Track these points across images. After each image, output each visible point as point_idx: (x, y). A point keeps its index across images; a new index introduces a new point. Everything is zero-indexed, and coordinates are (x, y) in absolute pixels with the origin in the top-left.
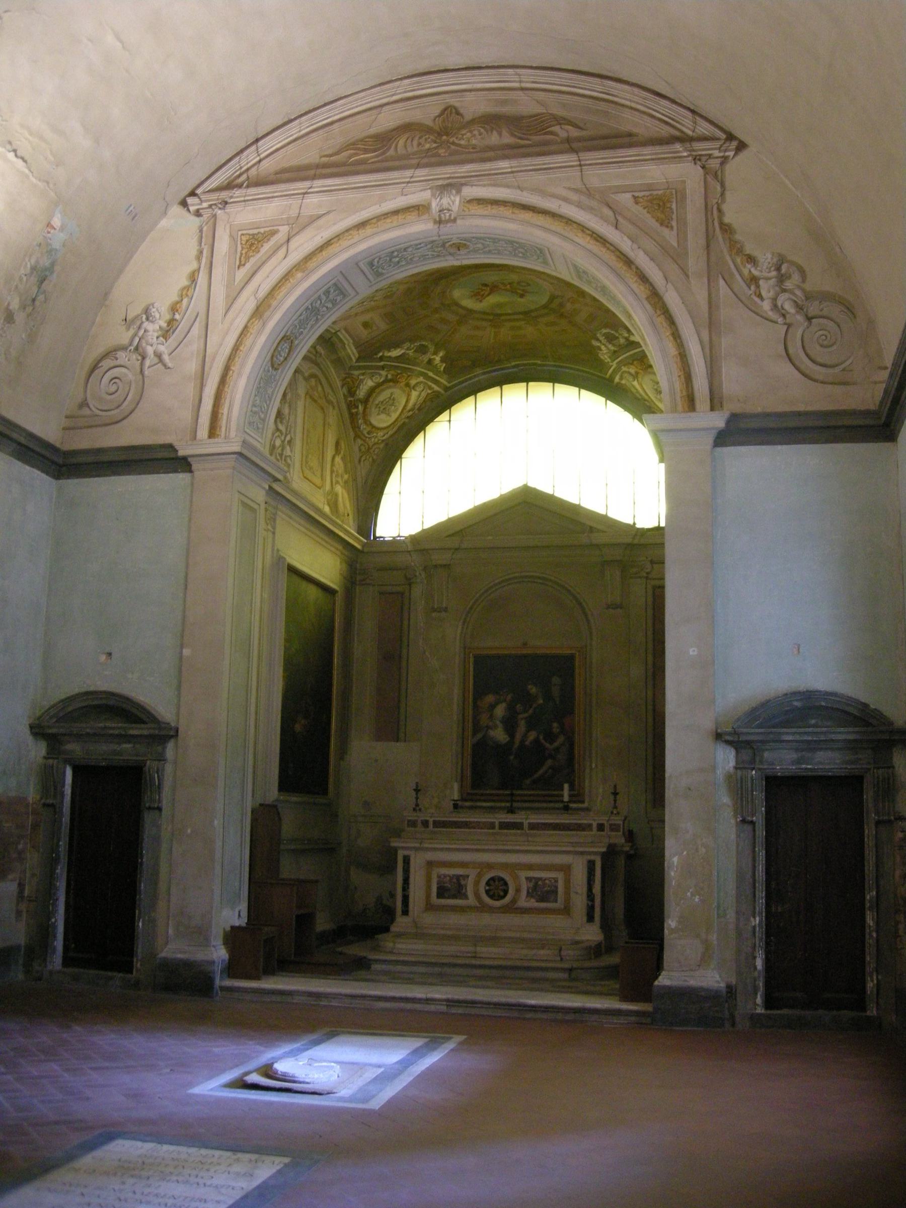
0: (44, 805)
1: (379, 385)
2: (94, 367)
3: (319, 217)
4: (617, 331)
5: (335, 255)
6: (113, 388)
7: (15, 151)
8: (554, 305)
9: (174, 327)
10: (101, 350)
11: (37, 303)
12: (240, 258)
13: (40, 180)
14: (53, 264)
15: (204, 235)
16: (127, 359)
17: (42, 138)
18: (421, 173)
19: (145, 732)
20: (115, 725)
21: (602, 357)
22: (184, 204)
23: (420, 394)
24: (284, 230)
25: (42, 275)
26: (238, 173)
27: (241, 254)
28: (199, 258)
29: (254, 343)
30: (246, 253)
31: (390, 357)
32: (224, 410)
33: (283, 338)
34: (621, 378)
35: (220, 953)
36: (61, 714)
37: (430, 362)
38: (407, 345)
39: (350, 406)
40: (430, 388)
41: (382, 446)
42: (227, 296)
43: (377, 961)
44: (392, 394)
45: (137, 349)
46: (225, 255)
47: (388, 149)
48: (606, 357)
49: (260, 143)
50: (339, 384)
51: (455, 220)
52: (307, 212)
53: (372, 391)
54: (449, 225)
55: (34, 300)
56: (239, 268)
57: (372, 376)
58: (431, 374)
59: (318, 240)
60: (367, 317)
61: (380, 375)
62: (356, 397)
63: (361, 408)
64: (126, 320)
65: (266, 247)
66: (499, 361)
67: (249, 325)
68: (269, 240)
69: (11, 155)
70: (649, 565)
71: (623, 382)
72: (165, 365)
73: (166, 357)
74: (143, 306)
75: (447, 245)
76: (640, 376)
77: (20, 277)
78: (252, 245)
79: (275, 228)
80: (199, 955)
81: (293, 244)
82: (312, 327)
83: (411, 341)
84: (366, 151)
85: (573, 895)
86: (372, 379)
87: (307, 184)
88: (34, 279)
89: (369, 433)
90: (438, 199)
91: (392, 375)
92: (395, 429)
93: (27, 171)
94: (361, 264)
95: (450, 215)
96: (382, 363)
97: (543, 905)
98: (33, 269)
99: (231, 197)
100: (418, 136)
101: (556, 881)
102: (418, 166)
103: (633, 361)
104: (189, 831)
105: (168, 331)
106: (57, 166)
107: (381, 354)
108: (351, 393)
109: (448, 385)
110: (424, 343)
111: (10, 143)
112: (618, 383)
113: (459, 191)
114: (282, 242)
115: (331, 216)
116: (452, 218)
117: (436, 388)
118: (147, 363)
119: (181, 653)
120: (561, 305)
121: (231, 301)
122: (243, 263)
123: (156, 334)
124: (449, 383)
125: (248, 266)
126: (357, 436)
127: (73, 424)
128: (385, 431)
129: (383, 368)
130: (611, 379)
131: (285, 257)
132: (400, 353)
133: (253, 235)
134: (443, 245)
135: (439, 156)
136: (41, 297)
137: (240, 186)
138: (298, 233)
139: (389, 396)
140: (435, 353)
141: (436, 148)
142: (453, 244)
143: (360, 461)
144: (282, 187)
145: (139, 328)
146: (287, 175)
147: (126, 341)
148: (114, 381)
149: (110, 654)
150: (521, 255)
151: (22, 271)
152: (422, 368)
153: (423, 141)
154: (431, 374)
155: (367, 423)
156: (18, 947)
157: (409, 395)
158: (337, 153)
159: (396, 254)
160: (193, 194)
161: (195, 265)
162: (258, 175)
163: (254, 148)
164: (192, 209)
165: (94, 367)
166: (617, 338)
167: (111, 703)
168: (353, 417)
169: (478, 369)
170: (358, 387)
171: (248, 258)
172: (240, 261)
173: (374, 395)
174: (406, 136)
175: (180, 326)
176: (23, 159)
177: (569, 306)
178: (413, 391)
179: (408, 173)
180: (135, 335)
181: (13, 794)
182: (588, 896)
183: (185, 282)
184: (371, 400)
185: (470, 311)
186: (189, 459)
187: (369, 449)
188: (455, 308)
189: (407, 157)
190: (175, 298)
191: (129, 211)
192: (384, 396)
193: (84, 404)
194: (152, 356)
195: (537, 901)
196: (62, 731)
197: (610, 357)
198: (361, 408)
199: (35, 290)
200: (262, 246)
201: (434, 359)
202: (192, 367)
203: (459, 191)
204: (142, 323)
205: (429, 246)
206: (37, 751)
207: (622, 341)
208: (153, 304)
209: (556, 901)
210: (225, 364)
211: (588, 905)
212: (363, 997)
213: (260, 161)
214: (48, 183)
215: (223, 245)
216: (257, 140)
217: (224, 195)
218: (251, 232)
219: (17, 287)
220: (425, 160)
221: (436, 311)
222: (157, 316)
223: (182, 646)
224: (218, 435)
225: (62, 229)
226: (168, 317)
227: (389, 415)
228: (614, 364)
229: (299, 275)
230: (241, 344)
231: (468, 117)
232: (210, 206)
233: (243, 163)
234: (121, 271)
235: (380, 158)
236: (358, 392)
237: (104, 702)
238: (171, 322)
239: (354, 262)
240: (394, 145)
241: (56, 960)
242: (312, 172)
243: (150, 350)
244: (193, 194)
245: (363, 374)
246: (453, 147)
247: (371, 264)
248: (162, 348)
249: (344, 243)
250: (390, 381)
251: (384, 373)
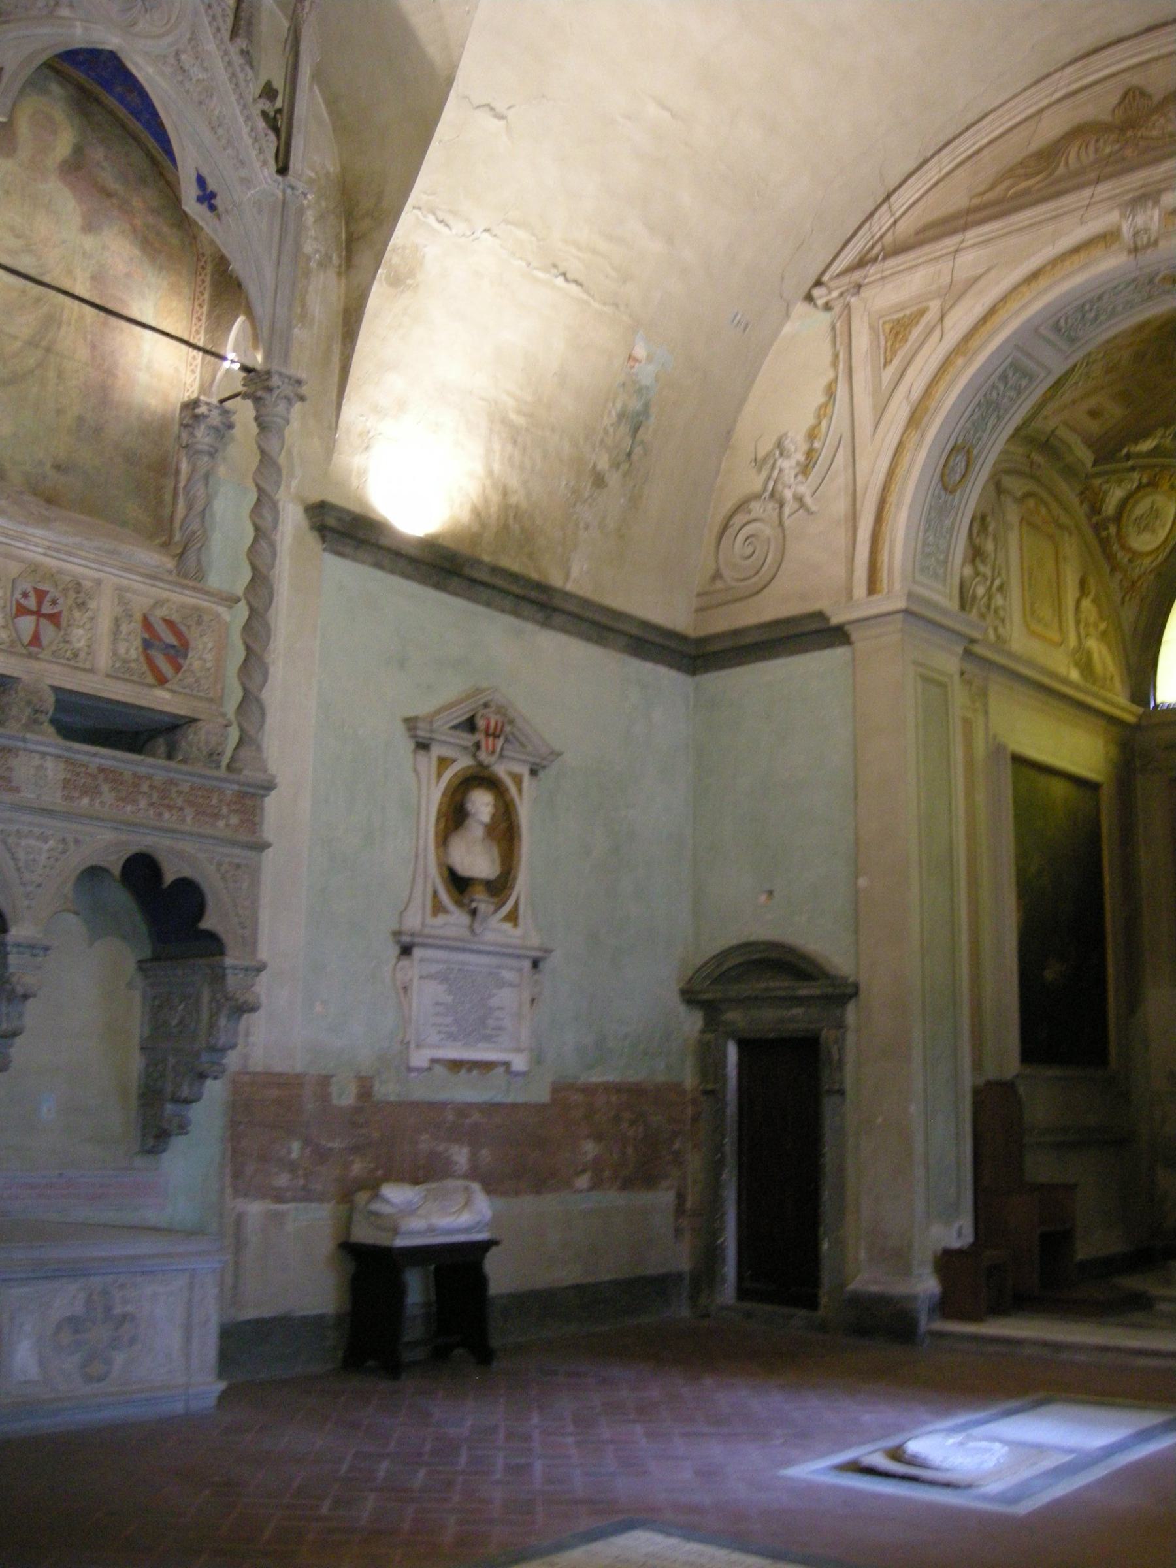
0: (706, 1093)
2: (725, 527)
3: (977, 279)
5: (1004, 324)
6: (749, 550)
7: (564, 274)
9: (814, 460)
10: (729, 505)
11: (634, 457)
12: (885, 353)
13: (605, 304)
14: (647, 406)
15: (838, 332)
16: (762, 510)
17: (594, 252)
18: (1104, 189)
19: (818, 992)
20: (779, 985)
22: (809, 298)
24: (935, 306)
25: (635, 422)
26: (870, 243)
27: (886, 349)
28: (835, 364)
29: (912, 462)
30: (892, 345)
32: (884, 557)
33: (952, 450)
35: (927, 1285)
36: (716, 974)
38: (1160, 432)
39: (1097, 528)
41: (1152, 577)
42: (874, 407)
43: (1165, 1299)
44: (1153, 504)
45: (772, 495)
46: (867, 353)
47: (1058, 165)
49: (893, 199)
50: (1076, 501)
51: (1156, 242)
52: (962, 275)
54: (1149, 251)
55: (629, 455)
56: (885, 365)
57: (1120, 482)
59: (979, 310)
60: (1092, 402)
62: (1104, 514)
63: (1112, 529)
64: (755, 459)
65: (916, 333)
67: (904, 438)
68: (917, 322)
69: (560, 281)
72: (809, 512)
73: (808, 500)
74: (774, 439)
75: (1157, 280)
77: (605, 429)
78: (897, 334)
79: (924, 305)
80: (899, 1288)
81: (948, 322)
82: (994, 427)
84: (1027, 177)
87: (957, 238)
88: (624, 429)
89: (1130, 561)
90: (1130, 219)
92: (1168, 550)
93: (585, 297)
94: (1043, 330)
95: (1149, 238)
96: (1130, 463)
98: (621, 416)
99: (865, 277)
100: (1093, 142)
102: (1098, 181)
104: (880, 1120)
105: (807, 466)
106: (624, 282)
107: (1125, 451)
108: (1095, 510)
111: (555, 266)
113: (1157, 202)
114: (932, 323)
115: (993, 274)
116: (1152, 239)
118: (787, 511)
119: (855, 884)
121: (880, 412)
122: (889, 358)
123: (793, 473)
125: (896, 362)
126: (1113, 570)
127: (707, 603)
128: (1154, 556)
129: (1133, 469)
131: (941, 340)
133: (898, 321)
134: (1151, 281)
135: (1124, 159)
136: (638, 450)
137: (875, 260)
138: (951, 307)
141: (1118, 151)
143: (1123, 603)
144: (927, 249)
145: (773, 468)
146: (930, 233)
147: (757, 486)
148: (748, 542)
149: (770, 893)
151: (606, 421)
153: (1101, 143)
155: (1124, 547)
156: (680, 1276)
158: (992, 187)
159: (1087, 307)
160: (818, 283)
161: (831, 374)
162: (894, 240)
163: (885, 207)
164: (820, 302)
165: (725, 527)
167: (774, 955)
168: (1104, 543)
170: (1103, 500)
171: (894, 352)
172: (885, 359)
173: (1128, 508)
174: (1077, 144)
175: (821, 458)
176: (576, 282)
179: (1087, 193)
180: (769, 478)
181: (661, 1078)
183: (821, 399)
184: (1125, 515)
186: (847, 628)
187: (1133, 584)
189: (1082, 171)
190: (811, 421)
191: (736, 322)
192: (1142, 507)
193: (717, 576)
194: (791, 501)
196: (719, 995)
198: (1112, 529)
199: (627, 444)
200: (910, 332)
202: (841, 507)
203: (1157, 202)
204: (775, 462)
205: (1132, 287)
206: (692, 1022)
208: (786, 434)
210: (879, 495)
212: (1118, 1350)
213: (895, 222)
214: (617, 306)
215: (862, 341)
216: (888, 197)
217: (857, 276)
218: (895, 316)
219: (602, 441)
220: (1109, 169)
222: (793, 449)
223: (857, 878)
224: (879, 592)
225: (650, 359)
226: (804, 447)
227: (1154, 531)
229: (960, 361)
230: (896, 465)
231: (1157, 98)
232: (841, 295)
233: (875, 228)
234: (742, 401)
235: (1047, 181)
237: (765, 955)
238: (810, 454)
239: (1032, 330)
240: (1063, 159)
241: (727, 1292)
242: (962, 221)
243: (788, 494)
244: (818, 283)
245: (1107, 482)
246: (1142, 144)
247: (1057, 328)
248: (802, 489)
249: (1013, 306)
250: (1149, 484)
251: (1136, 475)
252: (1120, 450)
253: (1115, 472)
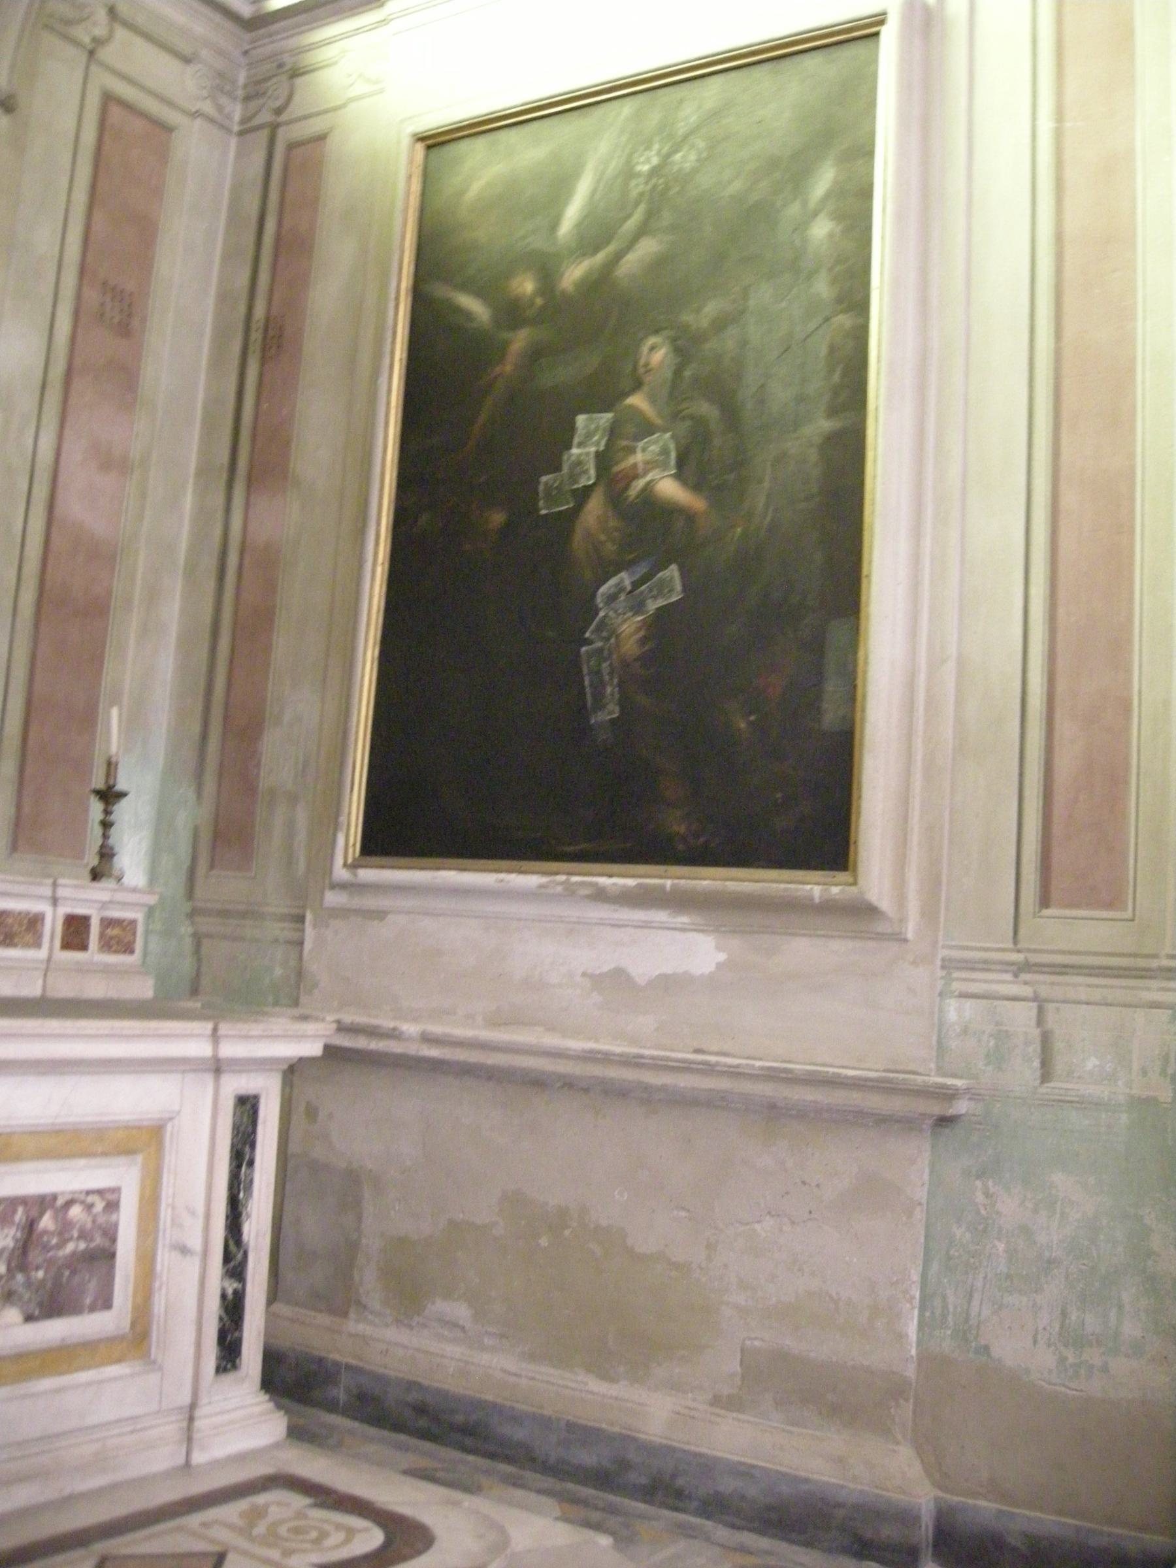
70: (101, 15)
85: (165, 1258)
97: (55, 1330)
101: (113, 1206)
182: (227, 1257)
195: (29, 1318)
209: (107, 1304)
211: (224, 1296)
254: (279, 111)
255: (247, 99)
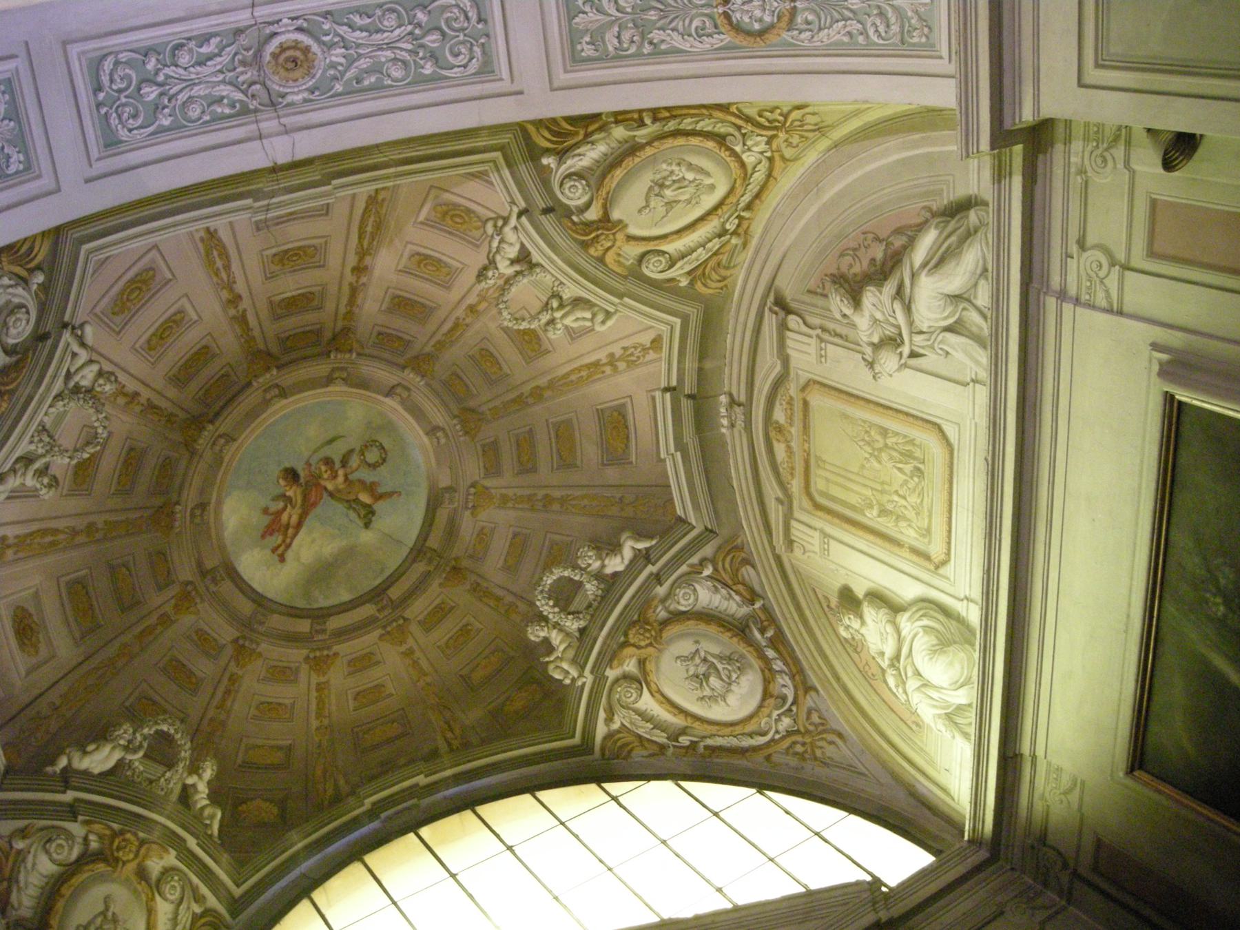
1: (70, 870)
4: (575, 567)
8: (433, 542)
21: (557, 676)
23: (176, 914)
31: (86, 773)
34: (609, 720)
37: (186, 795)
38: (125, 732)
40: (199, 899)
44: (107, 900)
48: (565, 666)
53: (54, 890)
58: (192, 843)
61: (70, 836)
66: (337, 799)
71: (616, 726)
76: (650, 666)
83: (135, 715)
86: (47, 852)
91: (101, 837)
96: (69, 796)
103: (626, 635)
107: (63, 762)
109: (237, 892)
110: (165, 728)
112: (609, 736)
117: (212, 901)
120: (452, 530)
124: (238, 886)
129: (72, 811)
130: (586, 746)
132: (110, 764)
139: (101, 908)
140: (194, 769)
142: (283, 48)
150: (428, 69)
152: (168, 817)
154: (192, 843)
157: (150, 912)
166: (580, 585)
169: (293, 835)
170: (12, 879)
173: (60, 905)
177: (467, 527)
178: (158, 898)
185: (258, 599)
188: (227, 587)
197: (574, 661)
201: (194, 786)
207: (591, 588)
221: (186, 598)
228: (588, 679)
236: (14, 897)
245: (23, 833)
250: (99, 856)
251: (77, 829)
252: (52, 762)
253: (40, 810)
254: (1065, 865)
255: (1045, 884)
